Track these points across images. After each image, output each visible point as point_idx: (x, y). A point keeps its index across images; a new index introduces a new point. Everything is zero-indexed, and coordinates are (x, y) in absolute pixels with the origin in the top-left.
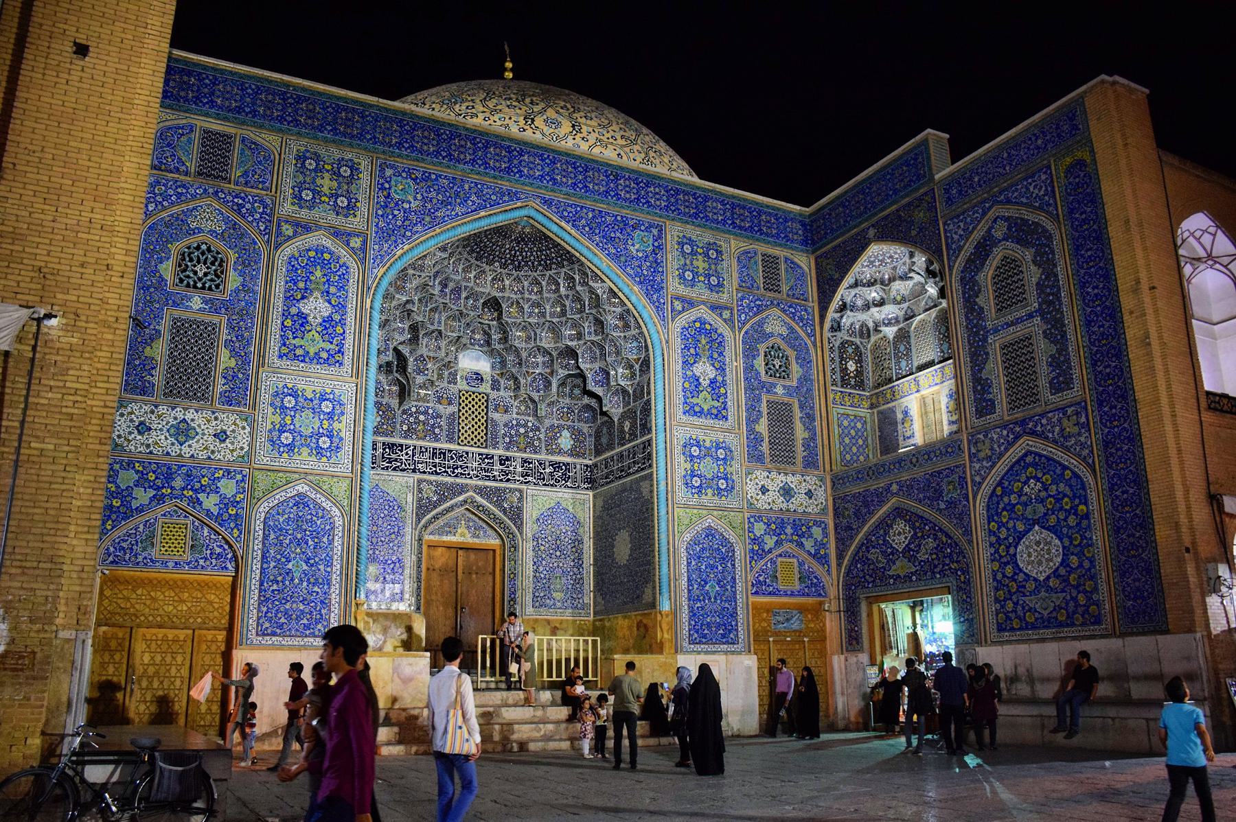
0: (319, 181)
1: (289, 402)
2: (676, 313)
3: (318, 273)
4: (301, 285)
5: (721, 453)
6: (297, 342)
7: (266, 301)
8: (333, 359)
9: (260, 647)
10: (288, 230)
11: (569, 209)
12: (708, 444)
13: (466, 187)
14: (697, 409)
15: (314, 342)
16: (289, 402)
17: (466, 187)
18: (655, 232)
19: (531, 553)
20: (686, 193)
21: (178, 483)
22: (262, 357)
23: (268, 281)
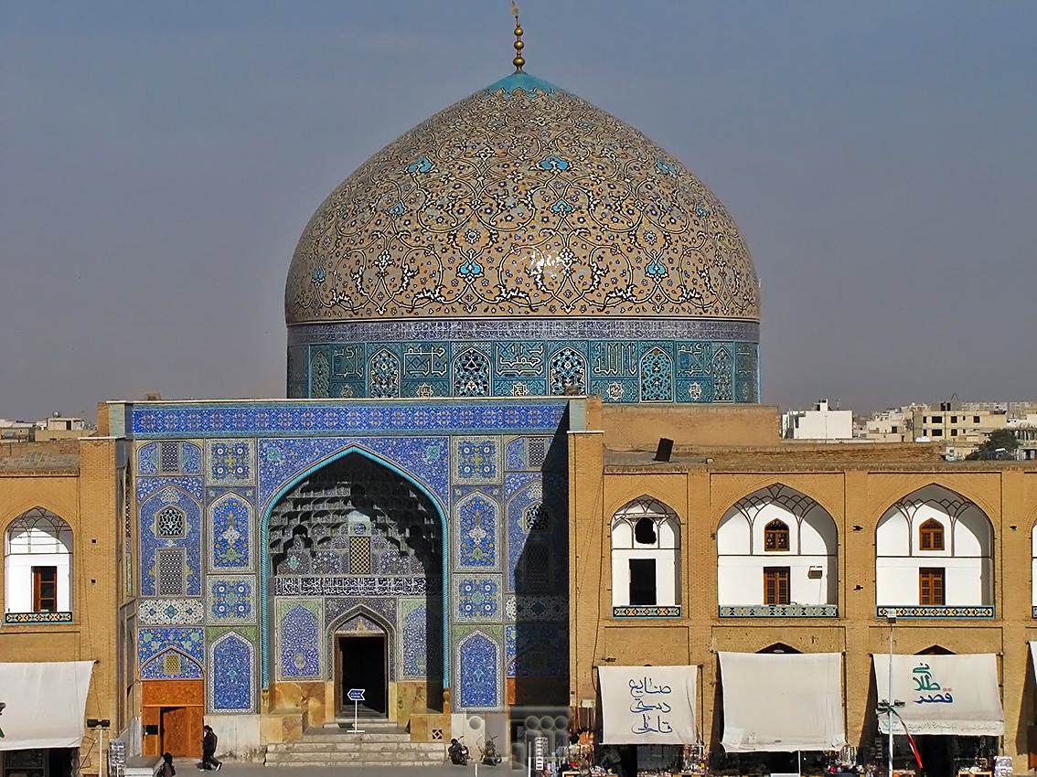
0: (226, 461)
1: (222, 589)
2: (455, 498)
3: (231, 515)
4: (222, 523)
5: (488, 588)
6: (223, 556)
7: (205, 536)
8: (243, 562)
9: (217, 714)
10: (212, 494)
11: (380, 442)
12: (478, 583)
13: (312, 444)
14: (471, 560)
15: (232, 555)
16: (222, 589)
17: (312, 444)
18: (442, 444)
19: (401, 640)
20: (465, 410)
21: (171, 638)
22: (206, 568)
23: (205, 526)
